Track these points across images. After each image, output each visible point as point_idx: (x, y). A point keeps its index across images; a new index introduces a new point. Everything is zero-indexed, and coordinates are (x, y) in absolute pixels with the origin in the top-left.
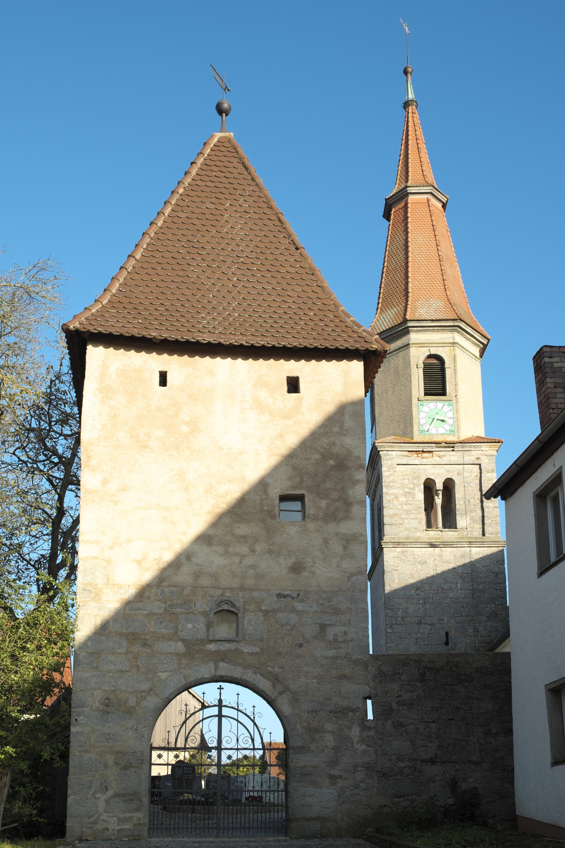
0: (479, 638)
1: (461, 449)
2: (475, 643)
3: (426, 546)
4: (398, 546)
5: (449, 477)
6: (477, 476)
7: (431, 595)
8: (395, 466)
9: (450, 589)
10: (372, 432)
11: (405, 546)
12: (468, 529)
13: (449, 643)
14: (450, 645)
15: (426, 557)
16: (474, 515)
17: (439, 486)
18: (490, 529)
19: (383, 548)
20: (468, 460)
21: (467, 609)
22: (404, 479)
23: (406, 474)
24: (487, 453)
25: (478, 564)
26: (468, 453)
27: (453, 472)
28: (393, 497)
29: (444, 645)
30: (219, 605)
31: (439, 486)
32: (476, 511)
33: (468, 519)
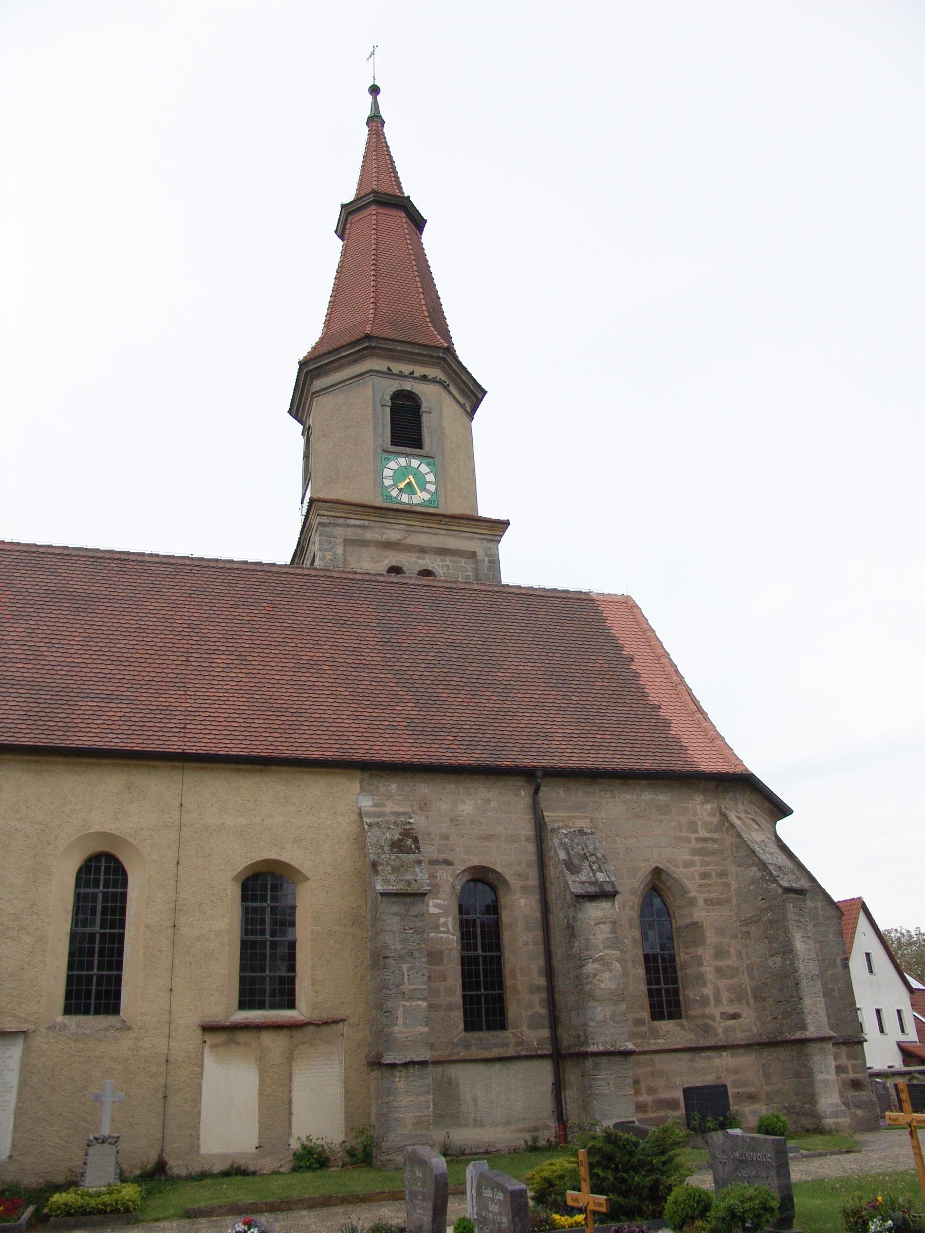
10: (302, 503)
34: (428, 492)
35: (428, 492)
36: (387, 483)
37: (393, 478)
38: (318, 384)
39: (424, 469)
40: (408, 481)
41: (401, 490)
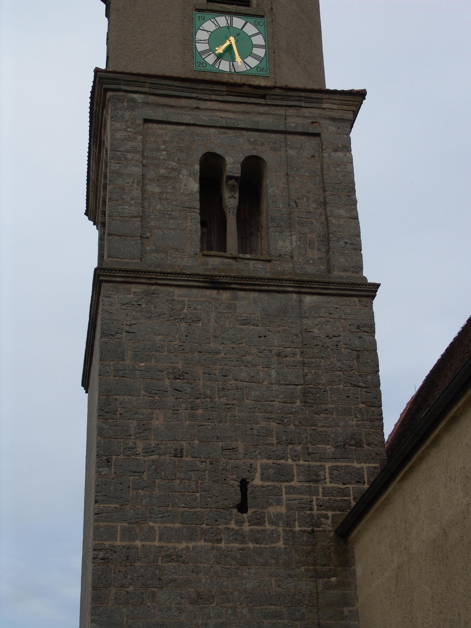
0: (320, 496)
2: (311, 509)
3: (201, 284)
4: (137, 280)
5: (254, 153)
6: (313, 156)
7: (208, 392)
8: (141, 122)
9: (253, 380)
11: (153, 281)
12: (296, 258)
13: (249, 505)
14: (250, 511)
15: (199, 307)
16: (306, 230)
18: (342, 260)
20: (293, 125)
21: (292, 427)
22: (158, 149)
23: (164, 142)
25: (316, 331)
27: (263, 144)
28: (131, 180)
29: (235, 510)
32: (312, 223)
33: (294, 237)
34: (256, 57)
35: (256, 57)
36: (201, 47)
37: (209, 41)
39: (250, 29)
40: (228, 43)
41: (219, 57)
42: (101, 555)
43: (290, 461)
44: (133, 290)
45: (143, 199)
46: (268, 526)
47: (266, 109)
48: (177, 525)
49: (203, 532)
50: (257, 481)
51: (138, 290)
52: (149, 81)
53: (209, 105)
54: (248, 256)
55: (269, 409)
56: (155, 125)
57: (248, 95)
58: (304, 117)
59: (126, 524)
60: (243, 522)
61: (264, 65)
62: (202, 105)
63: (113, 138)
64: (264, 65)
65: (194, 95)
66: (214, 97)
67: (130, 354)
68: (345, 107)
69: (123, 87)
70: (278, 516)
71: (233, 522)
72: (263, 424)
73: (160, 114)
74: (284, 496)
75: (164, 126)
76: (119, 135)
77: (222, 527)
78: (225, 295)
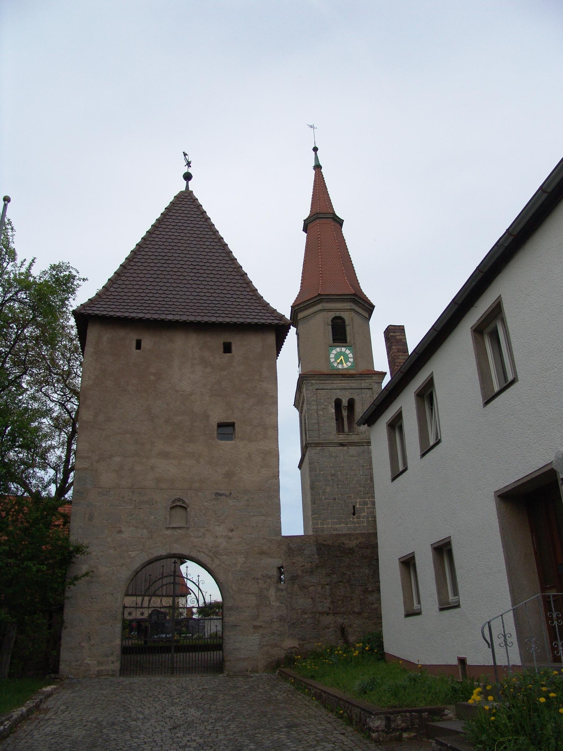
1: (358, 379)
8: (315, 390)
10: (299, 367)
12: (366, 433)
14: (356, 515)
17: (345, 403)
19: (308, 447)
21: (367, 489)
22: (321, 399)
24: (377, 381)
26: (363, 381)
30: (174, 502)
31: (345, 403)
34: (350, 362)
35: (350, 362)
36: (332, 360)
37: (335, 358)
38: (301, 315)
39: (348, 352)
41: (338, 363)
42: (315, 530)
43: (367, 499)
44: (317, 449)
45: (318, 417)
46: (362, 519)
47: (354, 381)
48: (336, 520)
49: (343, 522)
50: (358, 506)
51: (319, 449)
52: (317, 376)
53: (336, 381)
54: (351, 434)
55: (360, 484)
56: (319, 390)
57: (348, 377)
58: (367, 383)
59: (321, 521)
60: (354, 518)
61: (353, 365)
62: (334, 382)
63: (307, 397)
64: (353, 365)
65: (331, 379)
66: (337, 379)
67: (318, 469)
68: (380, 378)
69: (309, 379)
70: (365, 516)
71: (351, 519)
72: (359, 488)
73: (321, 386)
74: (366, 510)
75: (322, 390)
76: (309, 395)
77: (348, 520)
78: (345, 448)
